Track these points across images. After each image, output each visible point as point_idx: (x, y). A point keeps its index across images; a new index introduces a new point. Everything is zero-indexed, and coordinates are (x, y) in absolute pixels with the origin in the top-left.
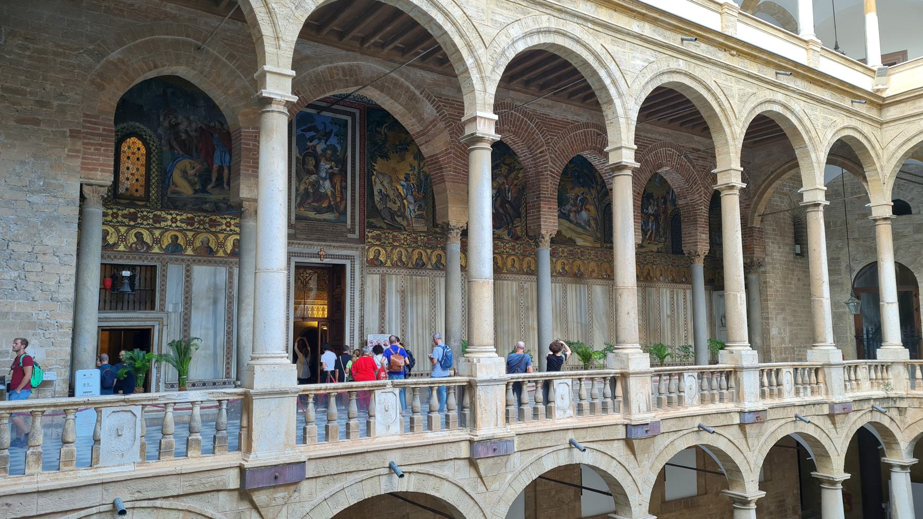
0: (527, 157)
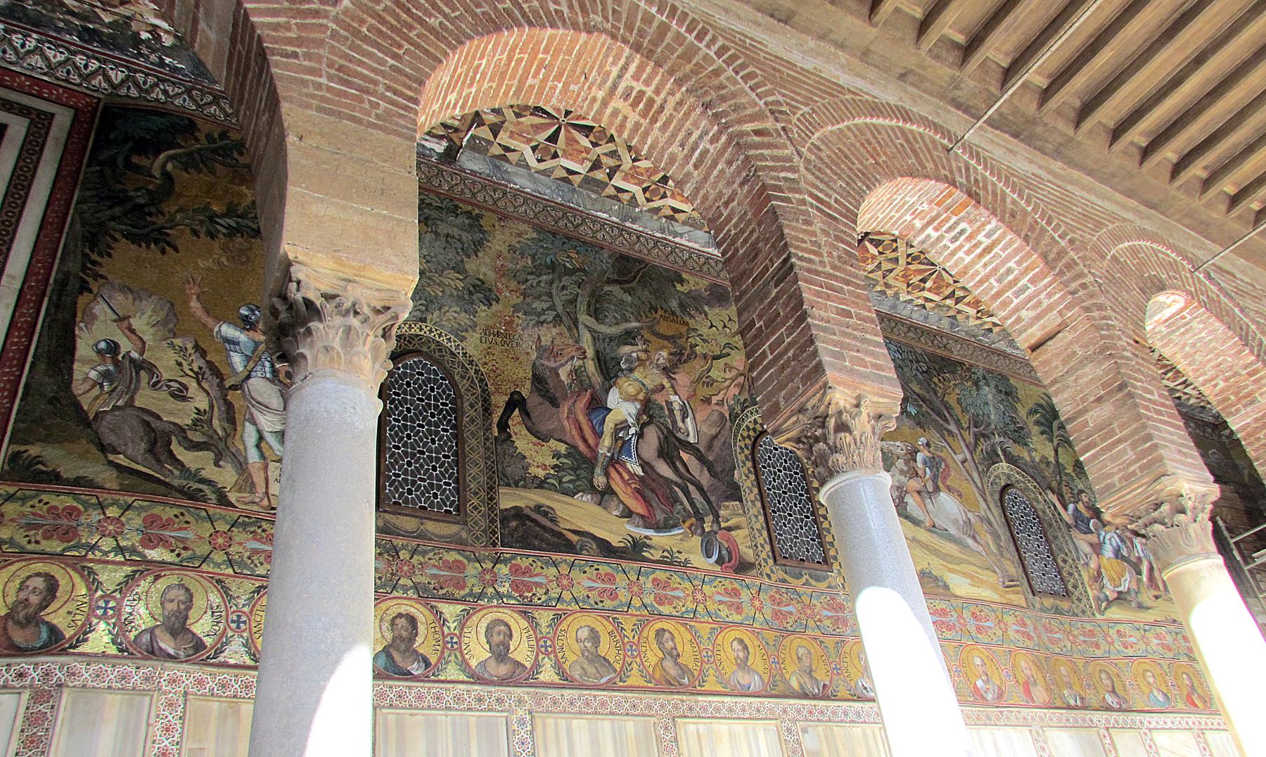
0: (708, 161)
